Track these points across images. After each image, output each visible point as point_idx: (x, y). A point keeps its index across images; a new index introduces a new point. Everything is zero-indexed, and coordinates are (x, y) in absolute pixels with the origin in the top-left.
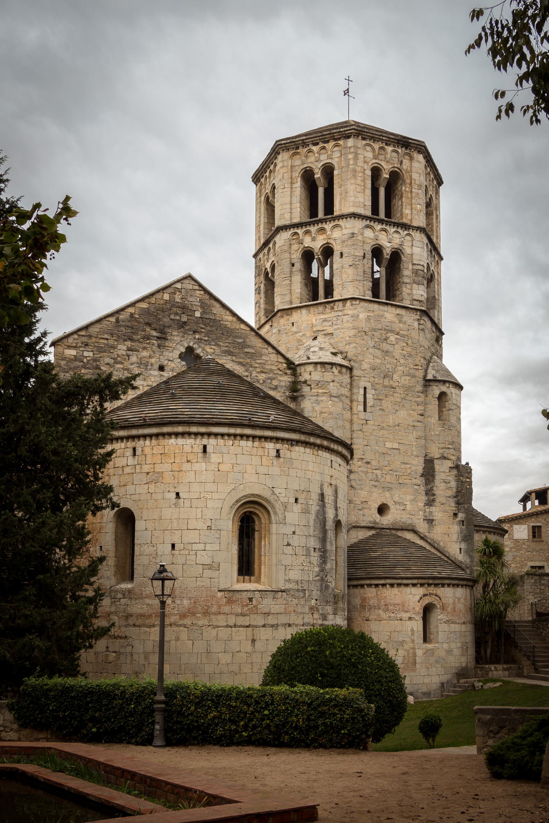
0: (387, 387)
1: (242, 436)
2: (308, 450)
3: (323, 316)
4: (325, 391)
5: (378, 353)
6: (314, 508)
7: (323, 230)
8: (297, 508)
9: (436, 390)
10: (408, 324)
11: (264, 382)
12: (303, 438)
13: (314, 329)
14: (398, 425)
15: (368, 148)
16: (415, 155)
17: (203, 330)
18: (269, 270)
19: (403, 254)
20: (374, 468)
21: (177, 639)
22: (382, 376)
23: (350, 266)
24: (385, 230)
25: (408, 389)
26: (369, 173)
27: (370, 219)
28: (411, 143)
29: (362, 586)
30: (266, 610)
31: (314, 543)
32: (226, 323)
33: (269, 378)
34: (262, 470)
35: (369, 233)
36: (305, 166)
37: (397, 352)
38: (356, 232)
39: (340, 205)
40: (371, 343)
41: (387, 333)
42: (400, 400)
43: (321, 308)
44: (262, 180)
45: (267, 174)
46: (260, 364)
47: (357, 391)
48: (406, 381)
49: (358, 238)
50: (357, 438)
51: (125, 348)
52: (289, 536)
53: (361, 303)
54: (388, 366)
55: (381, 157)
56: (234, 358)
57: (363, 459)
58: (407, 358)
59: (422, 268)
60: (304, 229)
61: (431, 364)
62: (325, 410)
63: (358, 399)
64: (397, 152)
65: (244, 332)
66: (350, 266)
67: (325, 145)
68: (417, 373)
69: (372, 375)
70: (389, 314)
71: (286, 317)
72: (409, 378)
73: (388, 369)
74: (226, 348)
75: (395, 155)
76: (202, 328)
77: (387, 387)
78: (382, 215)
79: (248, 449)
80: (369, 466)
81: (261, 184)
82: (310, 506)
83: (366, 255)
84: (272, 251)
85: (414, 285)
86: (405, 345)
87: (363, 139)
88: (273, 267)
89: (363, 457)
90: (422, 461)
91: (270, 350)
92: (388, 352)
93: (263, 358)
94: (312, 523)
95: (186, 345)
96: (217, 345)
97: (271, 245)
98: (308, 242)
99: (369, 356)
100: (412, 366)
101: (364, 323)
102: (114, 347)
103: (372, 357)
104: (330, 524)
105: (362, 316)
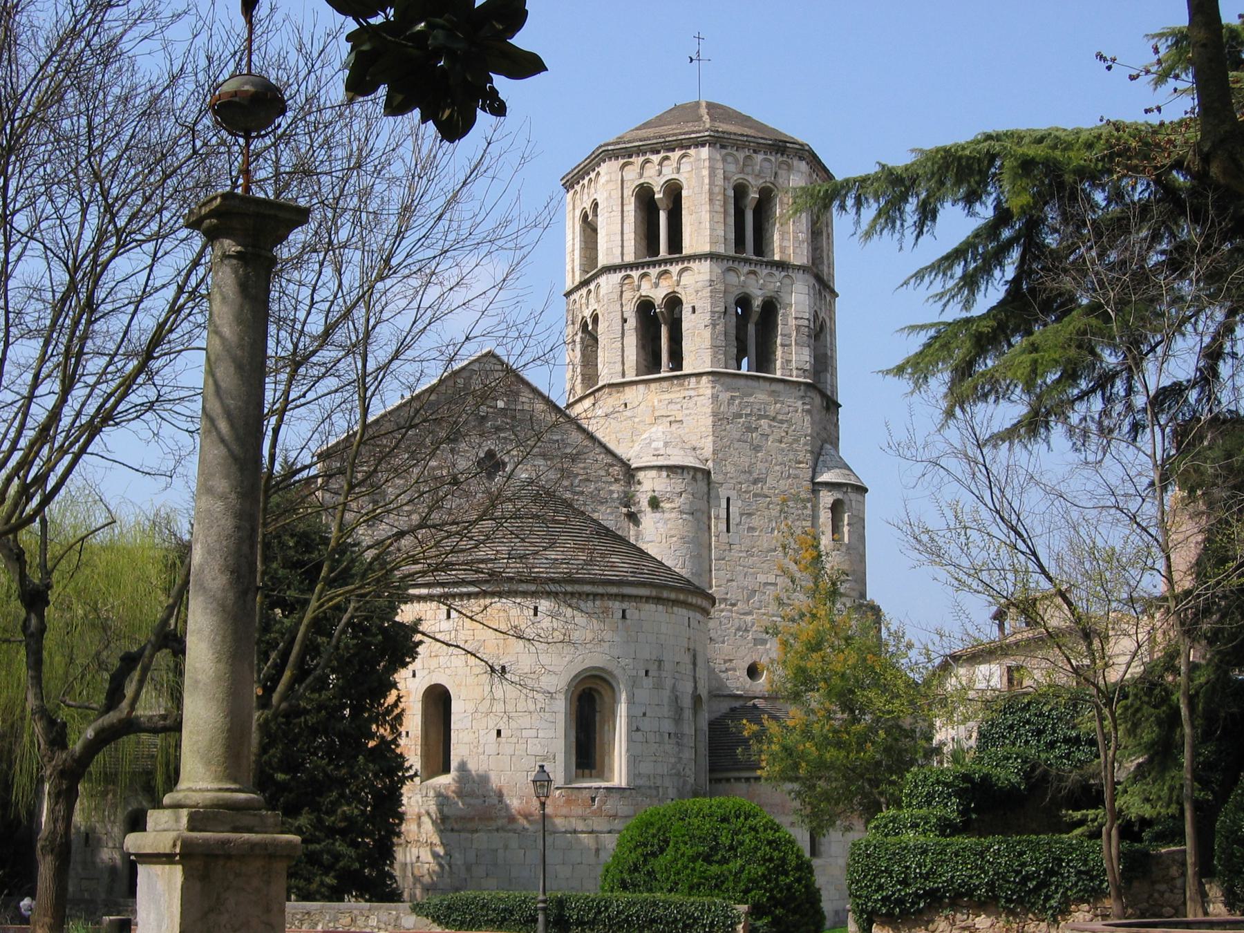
1: (581, 595)
2: (660, 607)
3: (666, 396)
4: (673, 505)
6: (668, 683)
8: (648, 683)
13: (657, 414)
15: (730, 159)
16: (796, 162)
18: (589, 321)
21: (506, 847)
24: (754, 273)
27: (734, 259)
29: (728, 780)
30: (612, 812)
31: (668, 726)
35: (732, 278)
36: (642, 181)
39: (691, 239)
43: (665, 384)
44: (578, 187)
45: (586, 181)
46: (584, 468)
55: (748, 169)
57: (725, 600)
59: (806, 323)
60: (641, 272)
61: (821, 458)
62: (672, 532)
64: (769, 161)
67: (669, 154)
70: (760, 396)
71: (615, 395)
75: (766, 164)
78: (749, 253)
81: (576, 192)
84: (592, 295)
87: (723, 147)
88: (595, 319)
94: (666, 701)
97: (592, 286)
98: (646, 289)
104: (687, 702)
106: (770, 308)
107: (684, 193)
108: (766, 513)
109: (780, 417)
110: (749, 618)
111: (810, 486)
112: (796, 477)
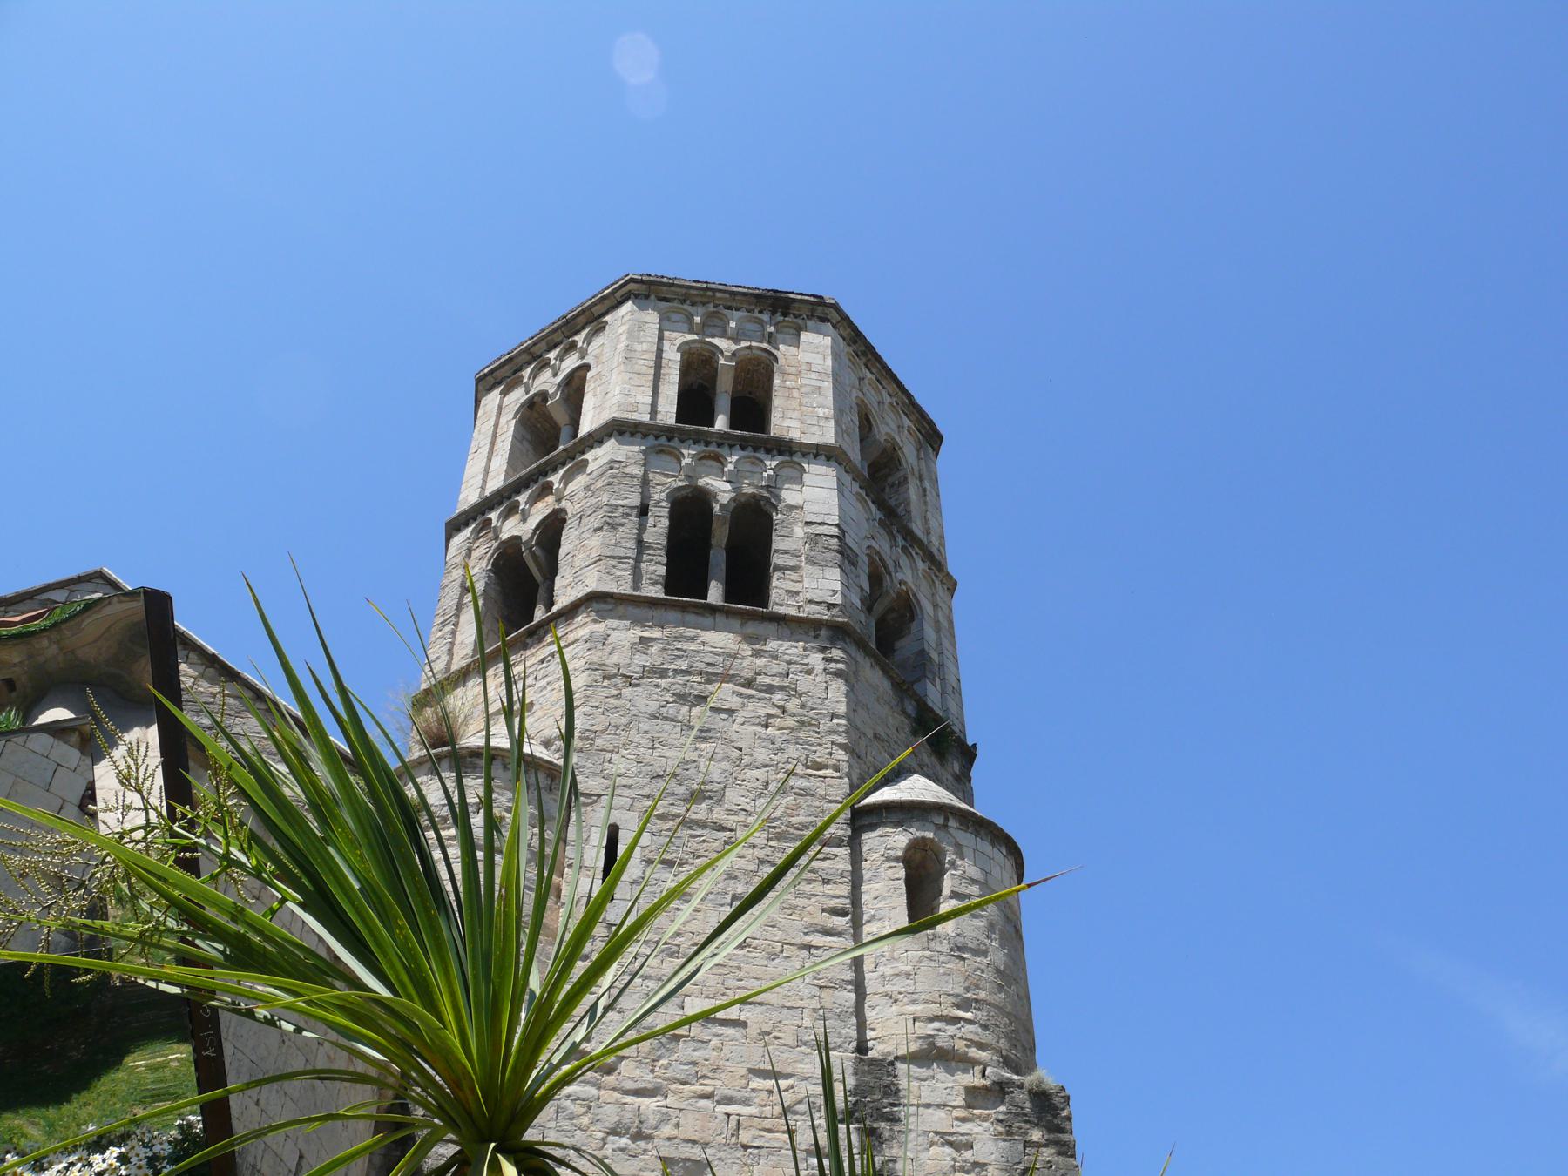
0: (703, 826)
7: (547, 489)
19: (775, 507)
20: (630, 1085)
22: (681, 790)
23: (596, 530)
26: (673, 357)
28: (794, 300)
41: (709, 682)
42: (752, 867)
49: (626, 470)
53: (621, 609)
58: (779, 744)
66: (596, 530)
69: (646, 791)
77: (703, 826)
83: (652, 510)
85: (807, 569)
86: (774, 711)
92: (709, 730)
99: (637, 738)
100: (800, 769)
103: (645, 742)
106: (755, 522)
107: (589, 375)
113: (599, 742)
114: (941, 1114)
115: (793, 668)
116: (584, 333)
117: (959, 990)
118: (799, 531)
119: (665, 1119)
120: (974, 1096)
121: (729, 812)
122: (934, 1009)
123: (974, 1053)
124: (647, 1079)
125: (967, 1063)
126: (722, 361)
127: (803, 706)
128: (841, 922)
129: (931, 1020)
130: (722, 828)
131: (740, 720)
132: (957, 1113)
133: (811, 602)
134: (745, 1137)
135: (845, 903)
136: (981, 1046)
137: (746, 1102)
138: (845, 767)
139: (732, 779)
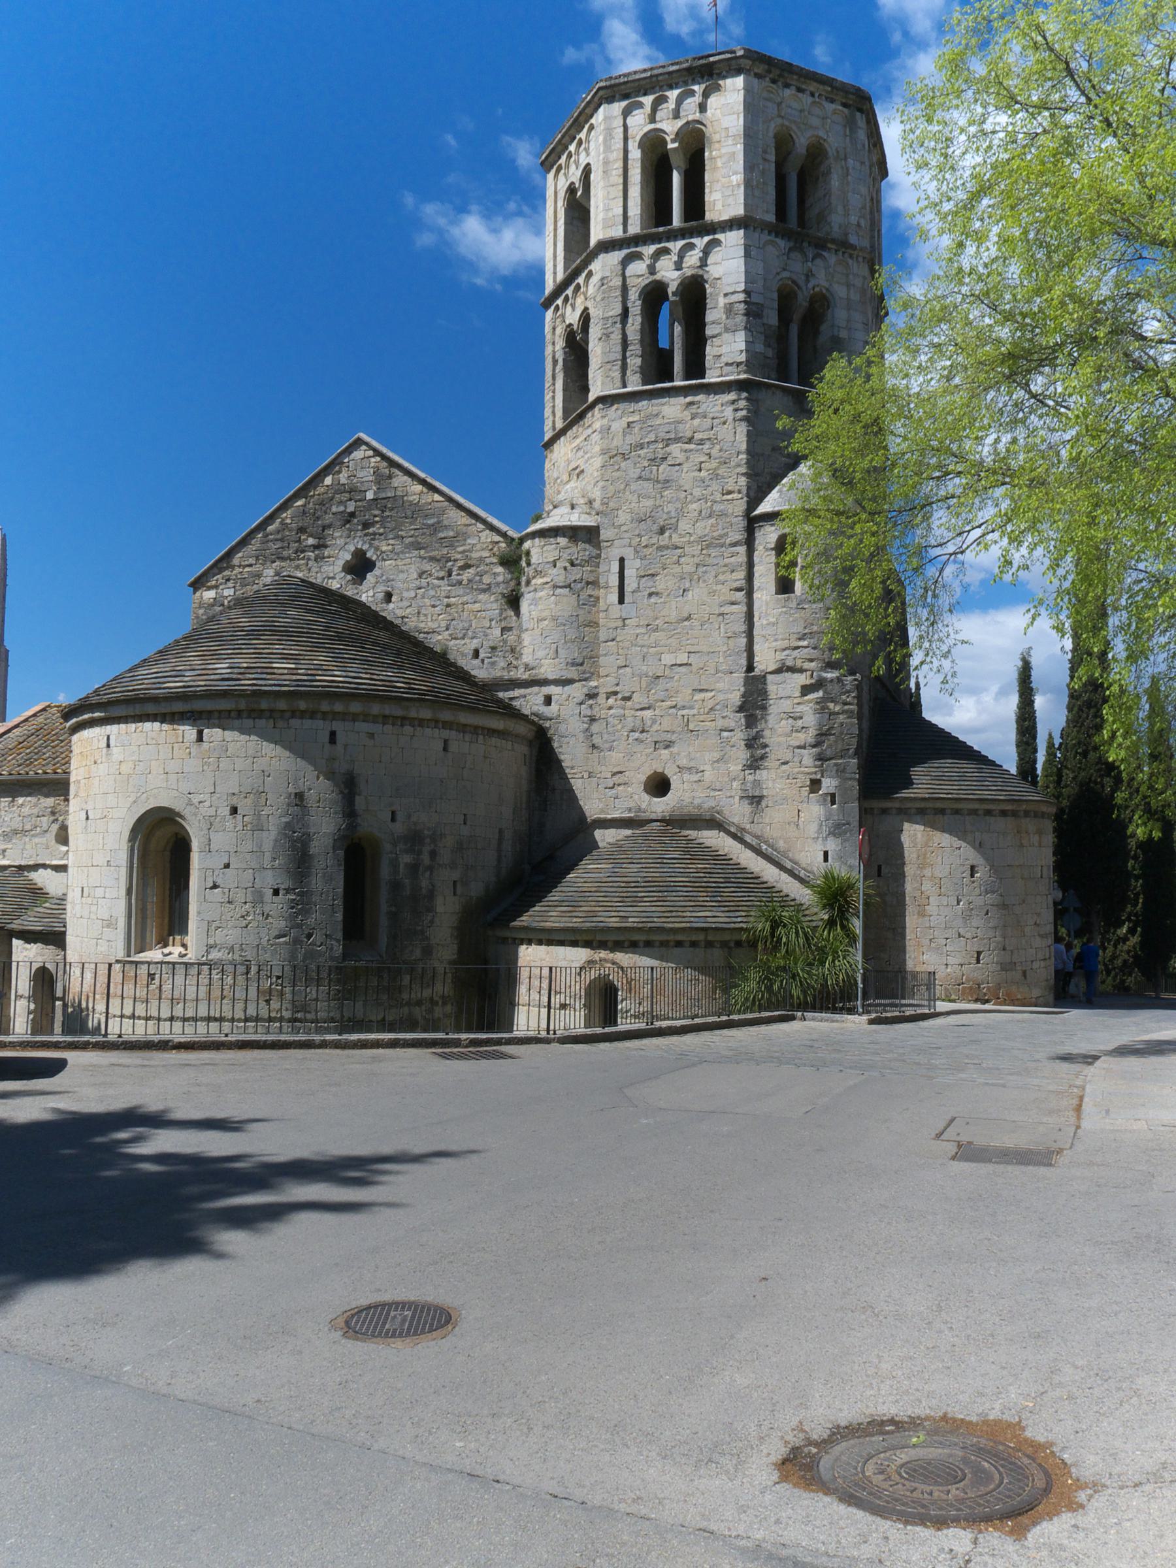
0: (667, 548)
5: (648, 485)
9: (768, 536)
10: (711, 415)
11: (470, 581)
12: (243, 705)
14: (688, 618)
17: (377, 519)
22: (655, 527)
24: (666, 251)
25: (708, 544)
26: (635, 154)
28: (715, 62)
32: (411, 498)
33: (477, 574)
34: (173, 766)
37: (687, 477)
38: (608, 274)
40: (634, 473)
41: (667, 445)
47: (606, 568)
48: (704, 527)
49: (611, 284)
50: (605, 655)
51: (271, 572)
52: (216, 873)
54: (670, 507)
56: (422, 552)
57: (616, 693)
63: (607, 583)
65: (439, 505)
68: (730, 508)
72: (713, 521)
73: (668, 513)
74: (411, 539)
76: (375, 516)
77: (667, 548)
79: (154, 734)
80: (629, 703)
82: (264, 818)
85: (726, 336)
87: (626, 97)
89: (617, 689)
90: (739, 677)
91: (480, 526)
92: (668, 481)
93: (469, 541)
94: (268, 845)
95: (353, 549)
96: (397, 537)
100: (718, 497)
101: (621, 438)
102: (259, 576)
105: (618, 426)
108: (677, 569)
109: (698, 436)
110: (647, 714)
111: (741, 523)
112: (723, 514)
113: (611, 504)
114: (788, 702)
115: (716, 422)
116: (585, 130)
117: (800, 629)
118: (722, 301)
119: (654, 722)
120: (806, 690)
121: (681, 536)
122: (786, 644)
123: (807, 665)
124: (645, 702)
125: (801, 671)
126: (670, 146)
127: (721, 450)
128: (740, 595)
129: (784, 650)
130: (677, 548)
131: (685, 470)
132: (796, 701)
133: (727, 364)
134: (691, 727)
135: (742, 583)
136: (811, 660)
137: (691, 708)
138: (744, 491)
139: (681, 513)
